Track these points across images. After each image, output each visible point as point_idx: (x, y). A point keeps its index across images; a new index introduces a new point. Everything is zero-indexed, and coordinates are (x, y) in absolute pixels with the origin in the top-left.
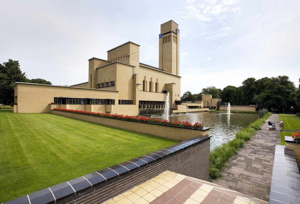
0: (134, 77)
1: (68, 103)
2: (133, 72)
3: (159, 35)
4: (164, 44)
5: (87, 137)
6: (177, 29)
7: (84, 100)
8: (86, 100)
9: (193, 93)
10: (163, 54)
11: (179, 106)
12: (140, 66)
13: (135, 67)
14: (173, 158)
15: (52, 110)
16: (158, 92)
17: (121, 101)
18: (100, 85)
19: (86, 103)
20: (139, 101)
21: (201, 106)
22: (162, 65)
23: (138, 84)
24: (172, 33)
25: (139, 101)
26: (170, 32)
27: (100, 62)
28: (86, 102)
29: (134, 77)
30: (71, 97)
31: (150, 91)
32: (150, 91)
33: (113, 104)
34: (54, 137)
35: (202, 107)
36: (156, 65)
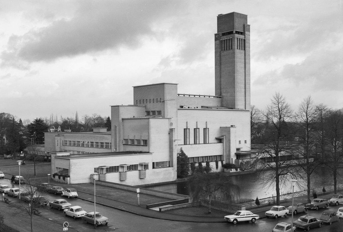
3: (216, 35)
16: (207, 143)
17: (155, 164)
26: (231, 33)
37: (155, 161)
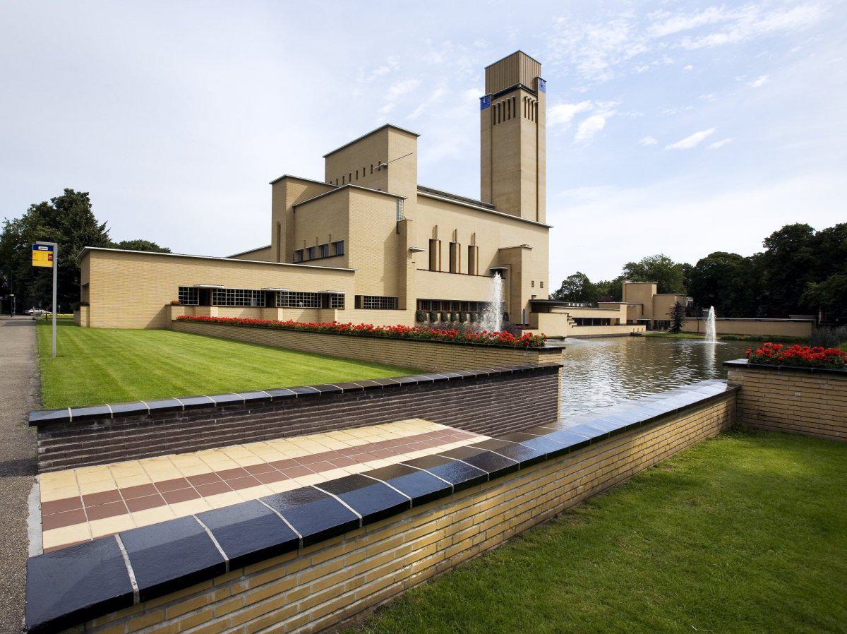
0: (401, 229)
1: (215, 303)
2: (398, 215)
3: (482, 99)
4: (497, 128)
5: (254, 369)
6: (536, 79)
7: (258, 296)
8: (263, 297)
9: (594, 280)
10: (494, 156)
11: (543, 317)
12: (419, 195)
13: (403, 199)
14: (433, 394)
15: (174, 321)
17: (362, 299)
18: (302, 254)
19: (263, 305)
20: (418, 301)
21: (618, 319)
22: (489, 194)
23: (412, 251)
24: (522, 92)
25: (418, 301)
26: (515, 88)
27: (303, 188)
28: (263, 300)
29: (401, 229)
30: (223, 287)
31: (452, 270)
32: (450, 272)
33: (340, 306)
34: (180, 366)
35: (621, 322)
36: (472, 189)
37: (362, 293)
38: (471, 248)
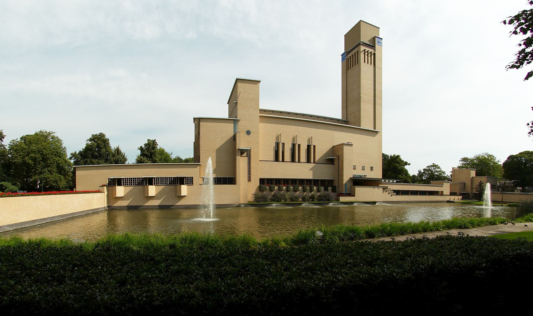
31: (293, 160)
38: (309, 147)
